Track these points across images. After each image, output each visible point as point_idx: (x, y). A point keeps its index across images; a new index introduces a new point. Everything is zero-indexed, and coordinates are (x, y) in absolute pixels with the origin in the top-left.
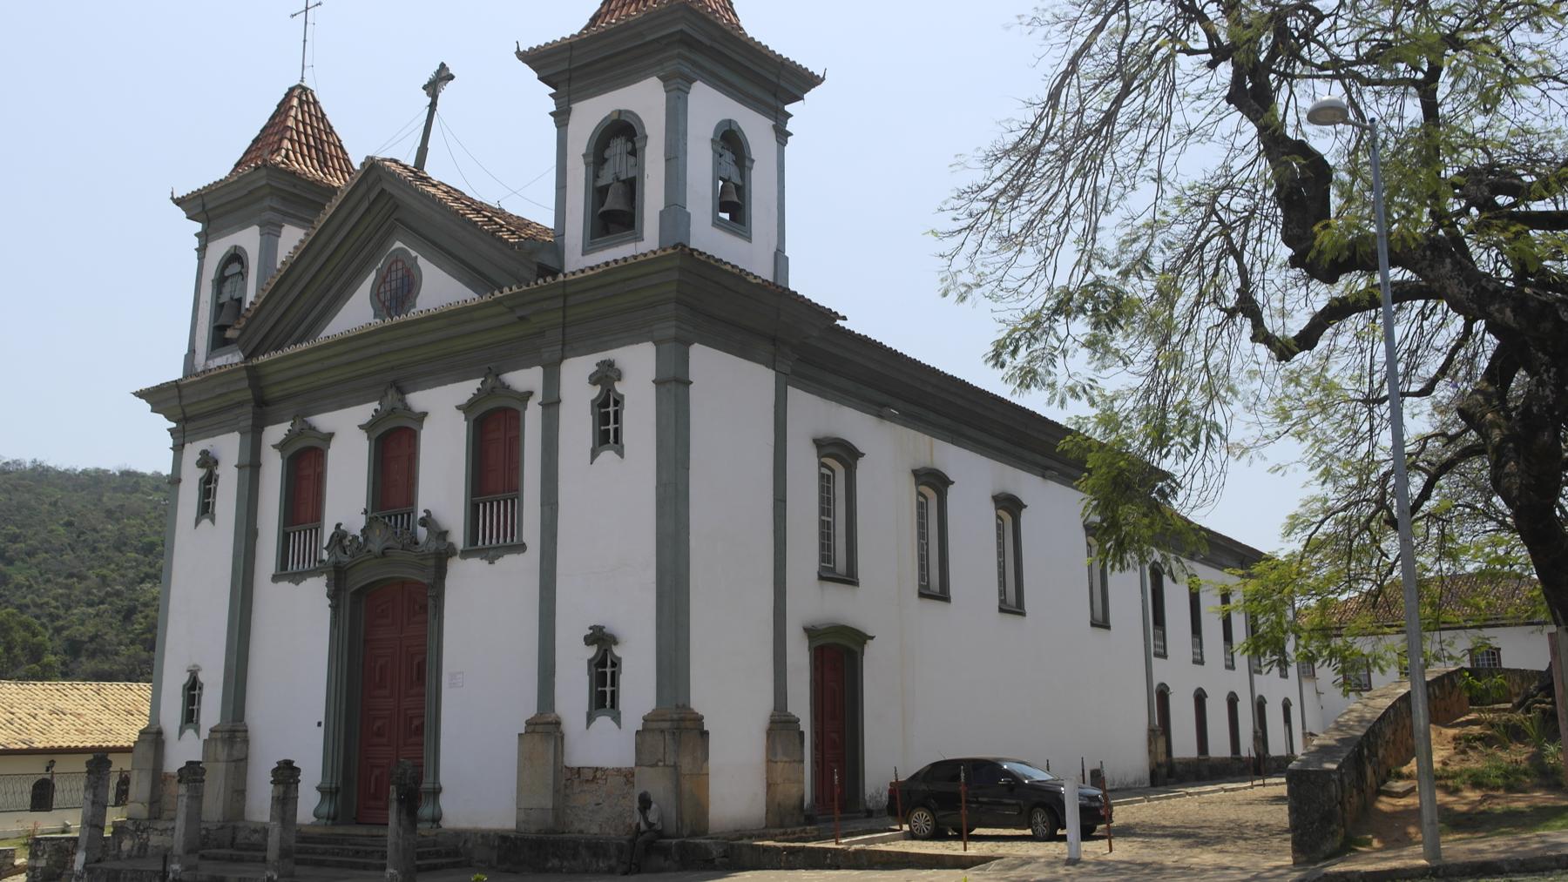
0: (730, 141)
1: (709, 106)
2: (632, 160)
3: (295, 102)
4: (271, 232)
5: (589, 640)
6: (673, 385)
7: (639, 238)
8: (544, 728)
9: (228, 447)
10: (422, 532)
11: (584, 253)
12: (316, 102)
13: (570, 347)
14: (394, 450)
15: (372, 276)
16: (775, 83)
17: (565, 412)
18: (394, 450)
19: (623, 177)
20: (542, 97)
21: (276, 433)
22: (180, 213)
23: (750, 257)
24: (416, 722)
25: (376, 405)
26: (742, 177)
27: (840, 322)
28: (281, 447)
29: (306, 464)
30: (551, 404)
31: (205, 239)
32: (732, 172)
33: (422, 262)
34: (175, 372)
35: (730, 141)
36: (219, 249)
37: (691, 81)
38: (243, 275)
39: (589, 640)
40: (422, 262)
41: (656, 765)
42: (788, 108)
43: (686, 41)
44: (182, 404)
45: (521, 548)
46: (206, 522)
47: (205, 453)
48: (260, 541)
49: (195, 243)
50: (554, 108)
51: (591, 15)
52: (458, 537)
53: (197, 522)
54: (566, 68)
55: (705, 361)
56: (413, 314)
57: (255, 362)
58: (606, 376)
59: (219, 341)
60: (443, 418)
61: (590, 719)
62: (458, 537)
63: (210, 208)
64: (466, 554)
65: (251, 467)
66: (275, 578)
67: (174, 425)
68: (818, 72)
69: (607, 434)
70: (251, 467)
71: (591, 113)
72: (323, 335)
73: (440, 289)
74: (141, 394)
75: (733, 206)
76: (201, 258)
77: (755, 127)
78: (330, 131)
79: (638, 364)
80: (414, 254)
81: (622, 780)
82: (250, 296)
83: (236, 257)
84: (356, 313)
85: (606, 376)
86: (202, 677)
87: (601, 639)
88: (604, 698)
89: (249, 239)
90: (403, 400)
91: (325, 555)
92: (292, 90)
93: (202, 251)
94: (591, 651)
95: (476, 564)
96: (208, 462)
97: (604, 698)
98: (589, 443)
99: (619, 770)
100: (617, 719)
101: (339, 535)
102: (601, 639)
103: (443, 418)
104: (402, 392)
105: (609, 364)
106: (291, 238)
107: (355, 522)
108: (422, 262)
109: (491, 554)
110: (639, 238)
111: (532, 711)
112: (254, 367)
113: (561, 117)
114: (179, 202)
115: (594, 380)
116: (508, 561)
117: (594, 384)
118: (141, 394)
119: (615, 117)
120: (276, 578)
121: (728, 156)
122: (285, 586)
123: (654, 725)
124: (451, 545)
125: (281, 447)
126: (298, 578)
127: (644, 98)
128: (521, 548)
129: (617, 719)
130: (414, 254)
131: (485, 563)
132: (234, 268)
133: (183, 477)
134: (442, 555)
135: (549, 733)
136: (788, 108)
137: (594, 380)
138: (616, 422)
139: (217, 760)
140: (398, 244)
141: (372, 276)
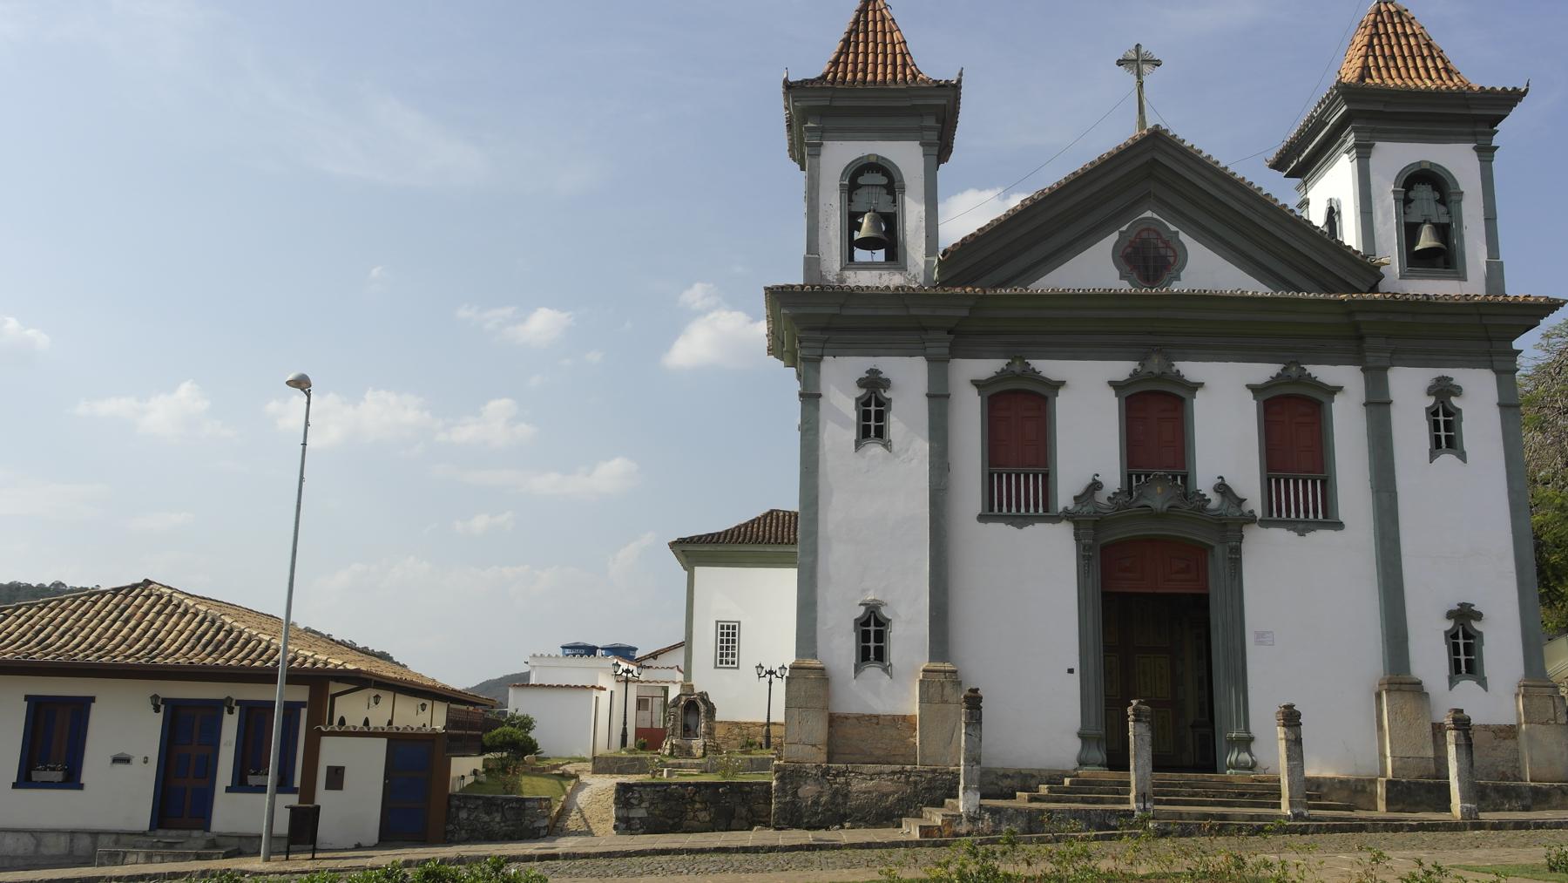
9: (907, 376)
10: (1215, 500)
15: (1114, 237)
17: (1396, 414)
30: (1378, 405)
33: (1183, 237)
40: (1184, 237)
41: (1547, 723)
47: (874, 372)
58: (1443, 392)
61: (1452, 682)
64: (1266, 523)
66: (982, 518)
70: (939, 399)
73: (1207, 271)
80: (1173, 228)
84: (1093, 270)
85: (1443, 392)
86: (885, 612)
94: (1449, 625)
99: (1486, 727)
105: (1448, 379)
107: (1113, 480)
109: (1302, 527)
116: (1321, 536)
117: (1429, 393)
120: (982, 518)
122: (999, 529)
130: (1173, 228)
139: (946, 702)
140: (1148, 214)
141: (1114, 237)
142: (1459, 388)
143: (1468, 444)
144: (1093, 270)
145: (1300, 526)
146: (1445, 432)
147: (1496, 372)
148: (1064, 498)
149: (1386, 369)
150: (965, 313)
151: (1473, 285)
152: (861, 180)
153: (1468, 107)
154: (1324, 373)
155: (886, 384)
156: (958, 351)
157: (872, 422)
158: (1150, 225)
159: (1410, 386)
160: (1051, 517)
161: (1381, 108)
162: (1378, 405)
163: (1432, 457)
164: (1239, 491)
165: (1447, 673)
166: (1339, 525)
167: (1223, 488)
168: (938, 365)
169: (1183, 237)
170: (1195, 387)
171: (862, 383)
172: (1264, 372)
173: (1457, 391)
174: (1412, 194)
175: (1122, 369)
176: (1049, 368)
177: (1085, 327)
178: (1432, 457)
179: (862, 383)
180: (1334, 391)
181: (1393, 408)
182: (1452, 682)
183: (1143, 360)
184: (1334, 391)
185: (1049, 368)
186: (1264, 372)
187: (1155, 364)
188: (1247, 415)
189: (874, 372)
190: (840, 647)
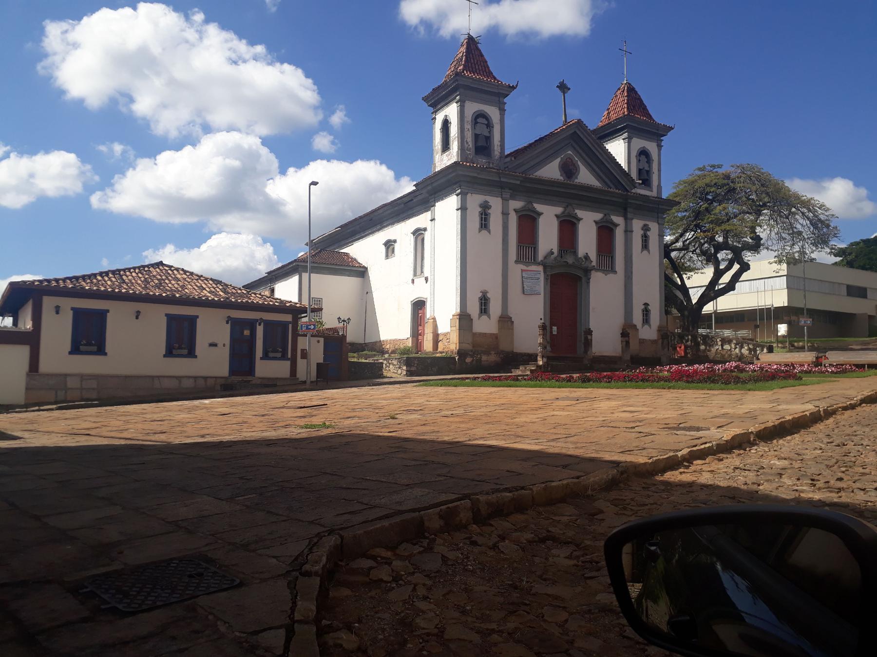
14: (568, 228)
15: (559, 159)
18: (568, 228)
30: (628, 231)
33: (579, 163)
58: (646, 228)
60: (588, 224)
64: (597, 270)
73: (585, 177)
85: (646, 228)
86: (489, 295)
88: (646, 320)
97: (646, 320)
103: (588, 224)
116: (611, 275)
133: (468, 206)
144: (551, 171)
148: (540, 257)
150: (518, 182)
151: (654, 193)
152: (478, 120)
155: (489, 207)
156: (513, 197)
157: (484, 224)
158: (570, 159)
159: (637, 225)
160: (535, 262)
162: (628, 231)
166: (615, 272)
169: (579, 163)
170: (579, 220)
171: (481, 206)
176: (539, 207)
177: (549, 191)
179: (481, 206)
180: (616, 225)
182: (643, 326)
184: (616, 225)
185: (539, 207)
188: (594, 230)
189: (486, 202)
190: (474, 309)
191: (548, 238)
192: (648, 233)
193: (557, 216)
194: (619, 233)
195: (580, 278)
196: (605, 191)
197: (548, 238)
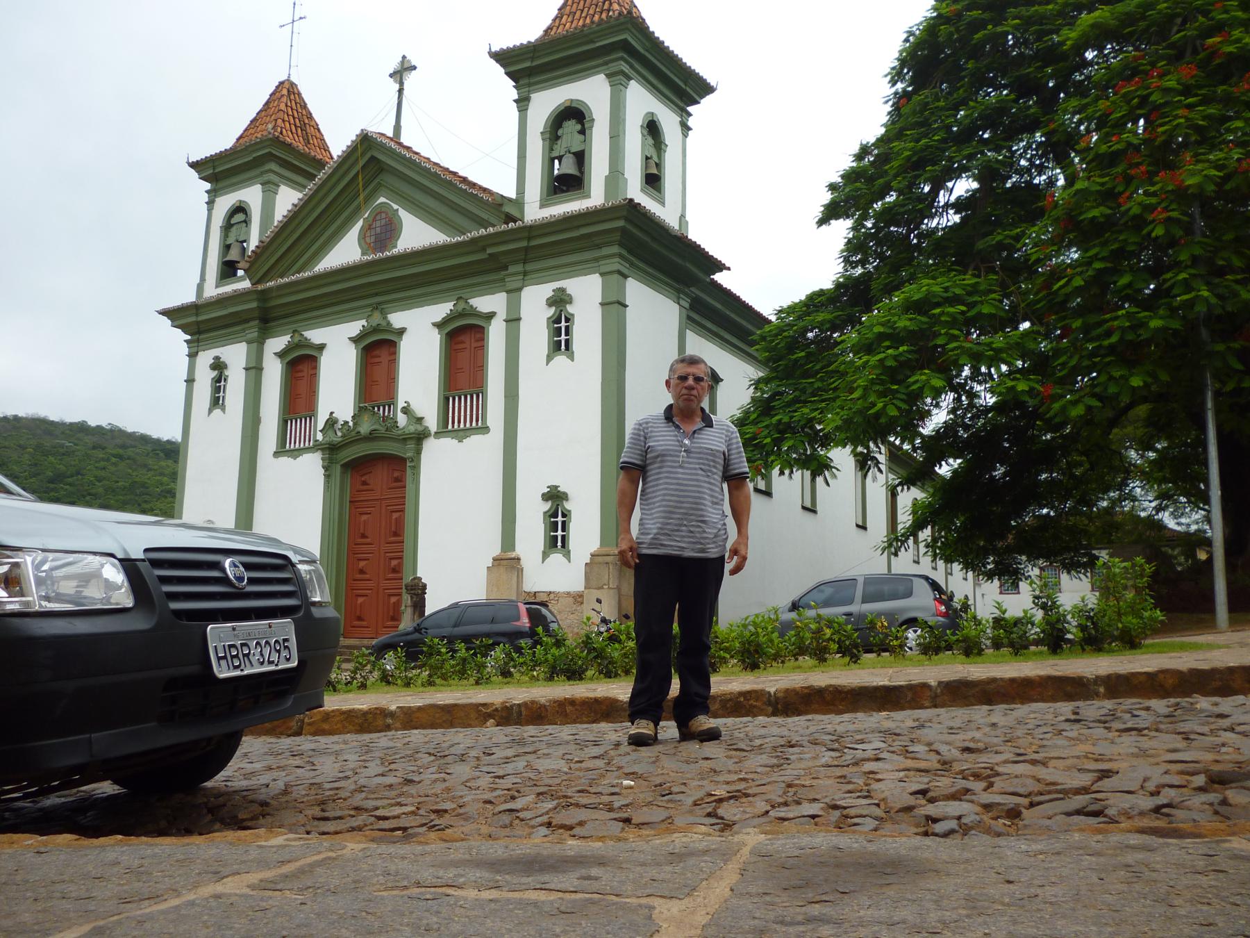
0: (652, 128)
1: (641, 101)
2: (582, 137)
3: (285, 92)
4: (270, 190)
5: (546, 497)
6: (614, 306)
7: (588, 196)
8: (507, 563)
9: (235, 355)
10: (402, 419)
11: (542, 206)
12: (299, 94)
13: (528, 277)
15: (360, 223)
16: (683, 87)
17: (524, 326)
19: (573, 150)
20: (508, 89)
21: (277, 343)
22: (193, 174)
23: (667, 214)
24: (394, 563)
25: (364, 322)
26: (659, 157)
27: (719, 277)
28: (281, 355)
29: (302, 366)
30: (513, 321)
31: (213, 195)
32: (652, 152)
34: (189, 297)
35: (652, 128)
36: (225, 202)
37: (629, 79)
38: (247, 222)
39: (546, 497)
40: (403, 214)
42: (690, 109)
43: (625, 46)
44: (200, 323)
45: (485, 429)
46: (217, 412)
47: (217, 358)
48: (262, 427)
49: (206, 197)
50: (516, 97)
51: (545, 27)
52: (432, 423)
53: (210, 411)
54: (527, 66)
55: (638, 293)
56: (395, 251)
57: (260, 287)
58: (560, 300)
59: (228, 270)
60: (420, 332)
62: (432, 423)
63: (218, 171)
64: (438, 435)
65: (255, 370)
66: (277, 454)
67: (189, 337)
68: (713, 83)
69: (560, 343)
70: (255, 370)
71: (547, 101)
72: (316, 269)
73: (416, 234)
74: (165, 313)
75: (653, 181)
76: (210, 210)
77: (668, 120)
78: (310, 116)
79: (586, 291)
80: (395, 207)
81: (571, 600)
82: (253, 243)
83: (240, 209)
84: (346, 251)
85: (560, 300)
87: (555, 496)
88: (557, 541)
89: (252, 195)
90: (385, 318)
91: (320, 437)
92: (281, 83)
93: (210, 203)
94: (547, 506)
95: (448, 443)
96: (219, 366)
97: (557, 541)
98: (544, 349)
99: (568, 593)
100: (567, 555)
101: (331, 422)
102: (555, 496)
103: (420, 332)
104: (384, 315)
105: (562, 290)
106: (287, 199)
108: (403, 214)
109: (461, 434)
110: (588, 196)
111: (496, 551)
112: (263, 291)
113: (522, 103)
114: (194, 165)
115: (551, 302)
116: (475, 440)
118: (165, 313)
119: (568, 104)
120: (277, 454)
121: (650, 141)
122: (285, 460)
123: (600, 559)
124: (427, 428)
125: (281, 355)
126: (295, 453)
127: (592, 91)
128: (485, 429)
129: (567, 555)
130: (395, 207)
131: (455, 441)
132: (239, 217)
134: (420, 437)
135: (513, 567)
136: (690, 109)
137: (551, 302)
138: (567, 334)
140: (382, 200)
141: (360, 223)
142: (570, 296)
143: (575, 346)
144: (346, 251)
145: (461, 434)
146: (560, 339)
147: (602, 274)
149: (520, 289)
150: (254, 305)
151: (596, 197)
153: (592, 42)
154: (483, 303)
159: (535, 300)
161: (527, 64)
163: (549, 359)
164: (419, 411)
165: (542, 548)
167: (406, 410)
168: (258, 345)
172: (442, 310)
173: (569, 300)
174: (560, 132)
175: (355, 327)
178: (549, 359)
180: (490, 316)
181: (522, 323)
183: (368, 318)
184: (490, 316)
186: (442, 310)
187: (377, 319)
191: (337, 392)
192: (570, 309)
193: (352, 339)
194: (496, 334)
195: (403, 461)
196: (458, 244)
197: (337, 392)
